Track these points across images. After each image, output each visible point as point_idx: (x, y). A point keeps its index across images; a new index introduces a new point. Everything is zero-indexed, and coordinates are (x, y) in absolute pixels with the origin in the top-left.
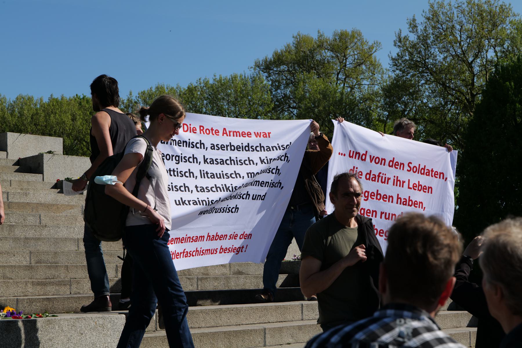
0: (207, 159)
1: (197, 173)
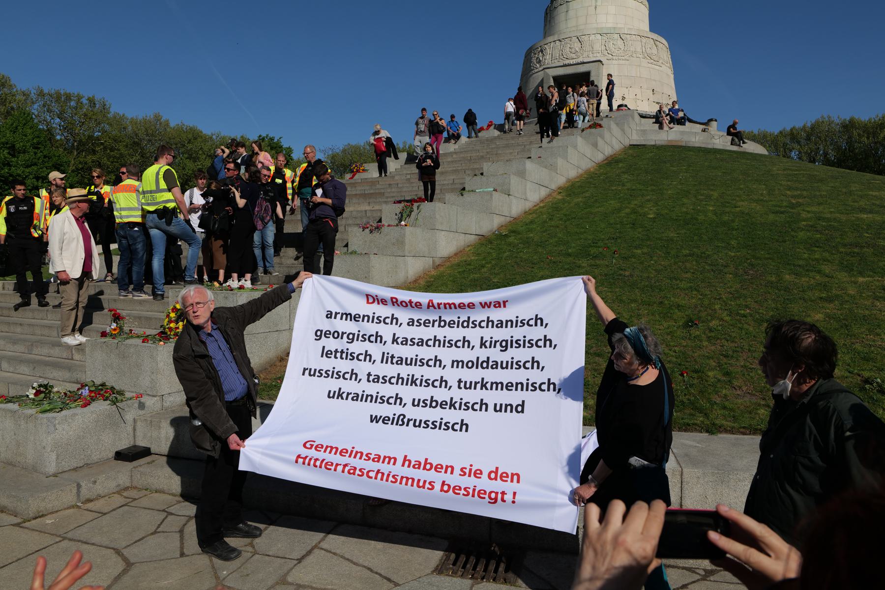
1: (377, 357)
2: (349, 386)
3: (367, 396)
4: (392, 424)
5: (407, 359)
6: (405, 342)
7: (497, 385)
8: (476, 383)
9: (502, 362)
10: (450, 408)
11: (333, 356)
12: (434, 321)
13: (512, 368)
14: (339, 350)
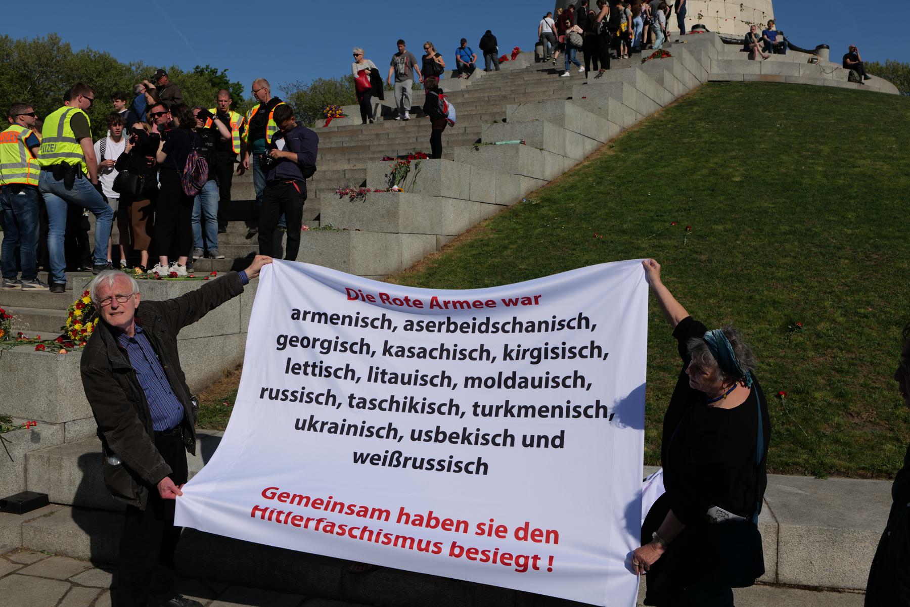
0: (391, 347)
1: (362, 372)
2: (325, 413)
3: (350, 426)
4: (384, 464)
5: (403, 375)
6: (401, 352)
7: (526, 410)
8: (498, 408)
9: (533, 379)
10: (463, 442)
11: (302, 372)
12: (441, 324)
13: (547, 386)
14: (311, 363)
